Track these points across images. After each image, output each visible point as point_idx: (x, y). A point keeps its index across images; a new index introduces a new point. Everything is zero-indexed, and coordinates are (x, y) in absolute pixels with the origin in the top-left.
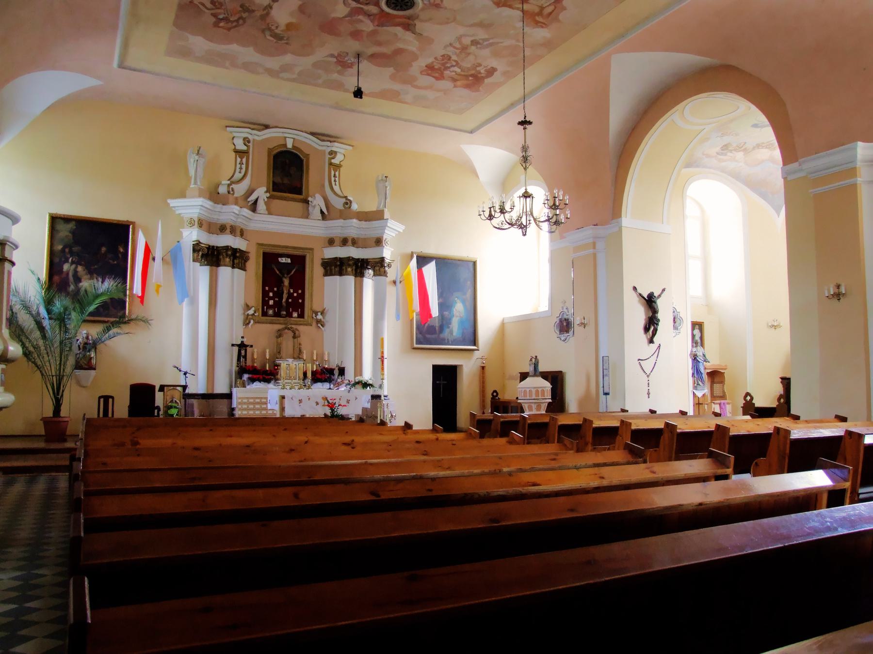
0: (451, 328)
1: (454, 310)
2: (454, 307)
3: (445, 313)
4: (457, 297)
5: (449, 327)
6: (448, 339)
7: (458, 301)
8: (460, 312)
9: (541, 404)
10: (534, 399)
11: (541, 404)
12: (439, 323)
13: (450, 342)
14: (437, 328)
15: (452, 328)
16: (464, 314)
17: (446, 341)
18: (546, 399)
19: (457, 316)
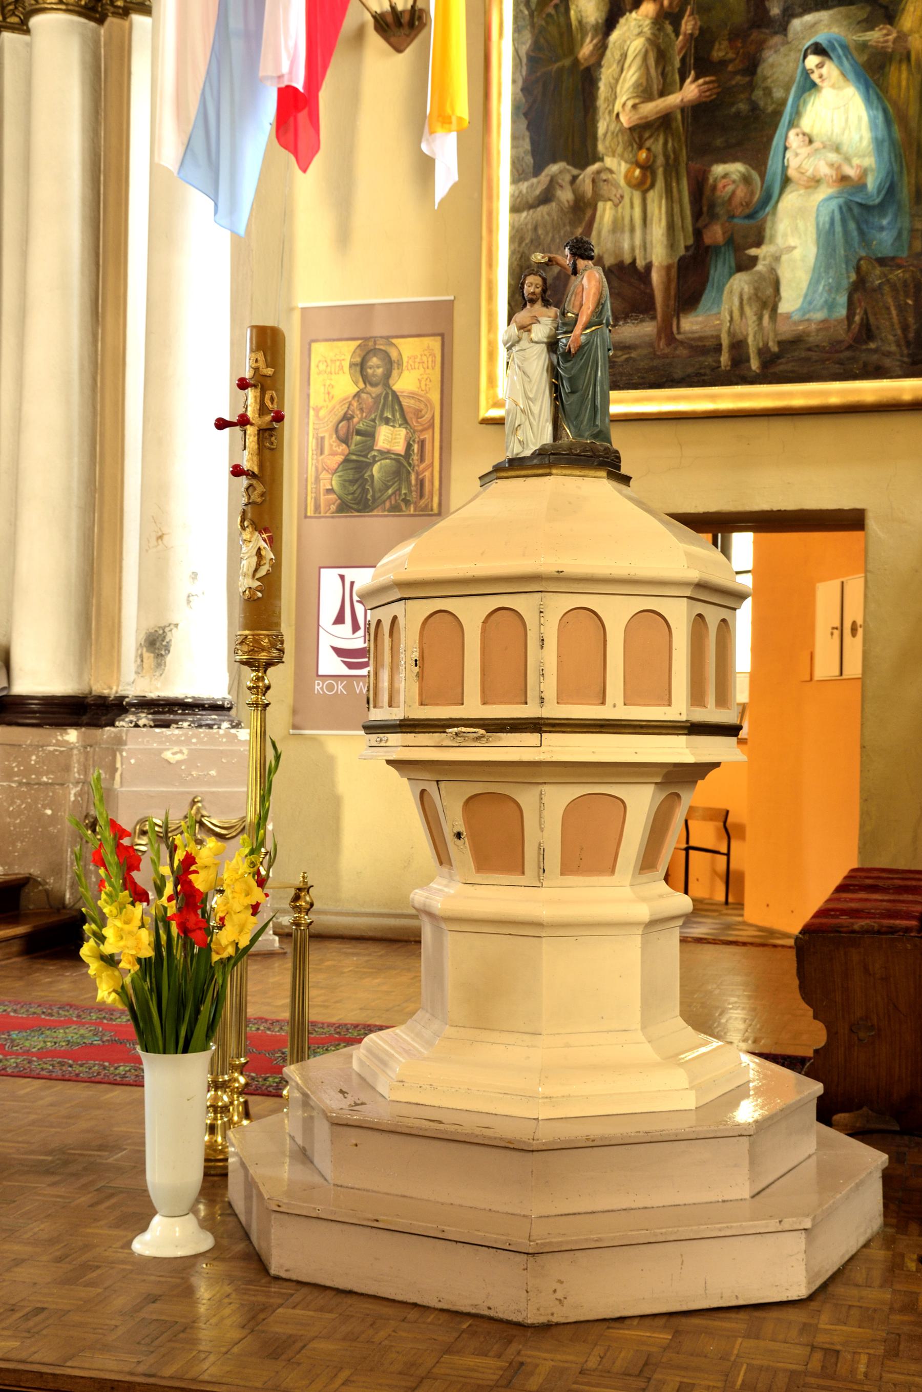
0: (760, 267)
1: (794, 139)
2: (792, 124)
3: (719, 169)
4: (818, 50)
5: (746, 264)
6: (738, 346)
7: (830, 70)
8: (837, 149)
9: (526, 798)
10: (407, 726)
11: (526, 798)
12: (672, 244)
13: (755, 364)
14: (656, 277)
15: (777, 259)
16: (869, 161)
17: (725, 359)
18: (536, 726)
19: (815, 182)
